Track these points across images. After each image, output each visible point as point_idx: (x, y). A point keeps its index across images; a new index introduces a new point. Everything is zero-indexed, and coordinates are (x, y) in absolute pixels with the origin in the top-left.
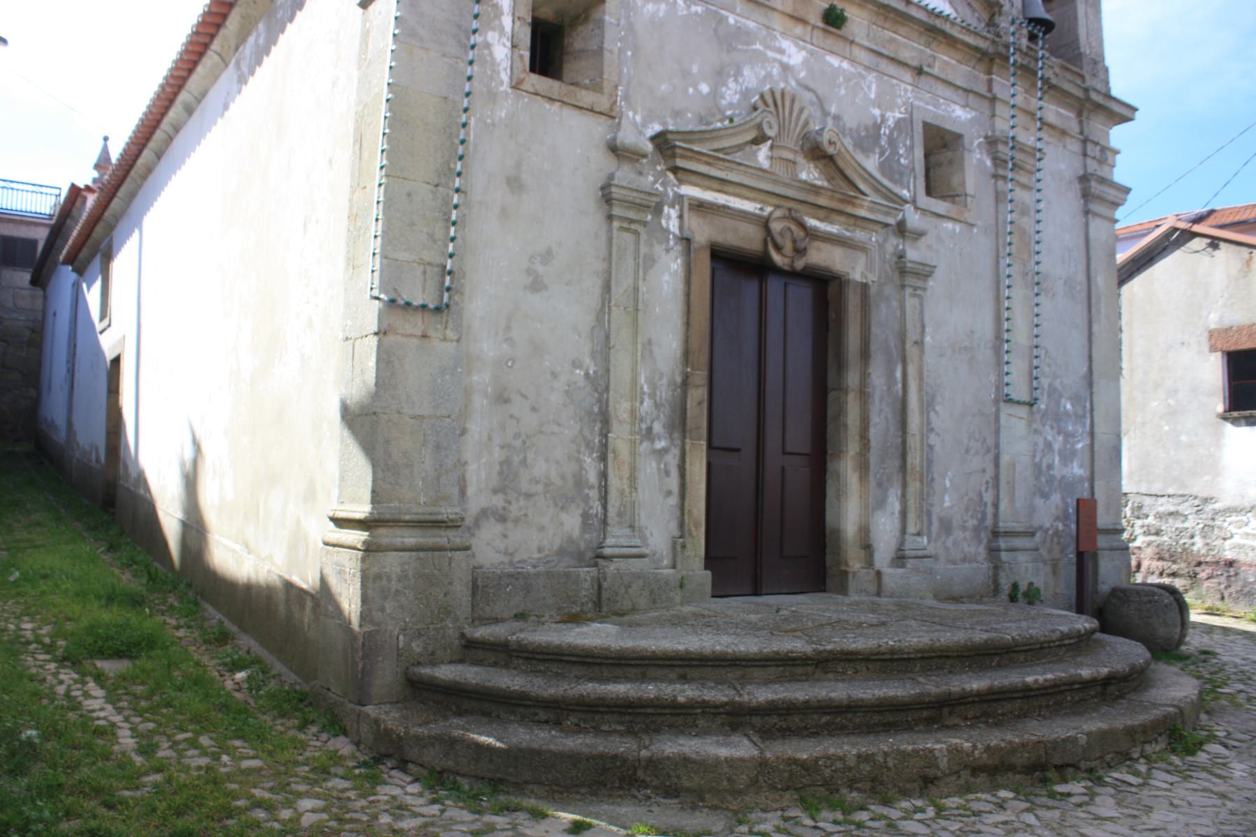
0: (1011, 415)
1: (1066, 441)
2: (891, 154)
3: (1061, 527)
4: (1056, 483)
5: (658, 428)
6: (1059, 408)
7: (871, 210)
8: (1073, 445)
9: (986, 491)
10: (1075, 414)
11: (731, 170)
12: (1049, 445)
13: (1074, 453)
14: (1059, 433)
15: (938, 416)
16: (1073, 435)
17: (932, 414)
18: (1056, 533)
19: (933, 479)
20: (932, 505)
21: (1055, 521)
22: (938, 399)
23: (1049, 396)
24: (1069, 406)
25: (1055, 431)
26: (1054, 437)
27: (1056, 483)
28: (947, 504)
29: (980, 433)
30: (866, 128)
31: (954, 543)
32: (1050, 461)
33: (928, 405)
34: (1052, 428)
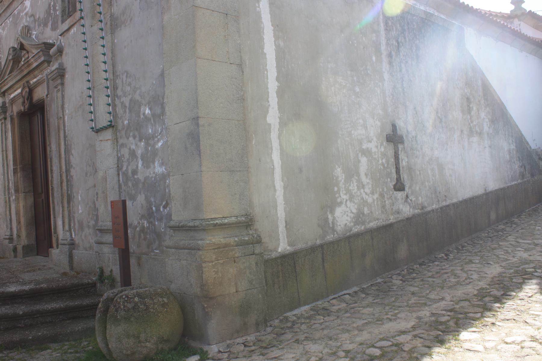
0: (101, 141)
1: (147, 144)
2: (54, 14)
3: (146, 224)
4: (140, 186)
5: (13, 192)
6: (139, 116)
7: (36, 61)
8: (153, 146)
9: (97, 200)
10: (154, 115)
11: (8, 83)
12: (133, 154)
13: (155, 153)
14: (140, 140)
15: (73, 157)
16: (153, 137)
17: (71, 156)
18: (143, 230)
19: (74, 196)
20: (74, 213)
21: (141, 219)
22: (73, 146)
23: (130, 111)
24: (147, 111)
25: (137, 139)
26: (136, 145)
27: (140, 186)
28: (80, 211)
29: (91, 160)
30: (47, 11)
31: (85, 237)
32: (135, 167)
33: (68, 151)
34: (134, 137)
